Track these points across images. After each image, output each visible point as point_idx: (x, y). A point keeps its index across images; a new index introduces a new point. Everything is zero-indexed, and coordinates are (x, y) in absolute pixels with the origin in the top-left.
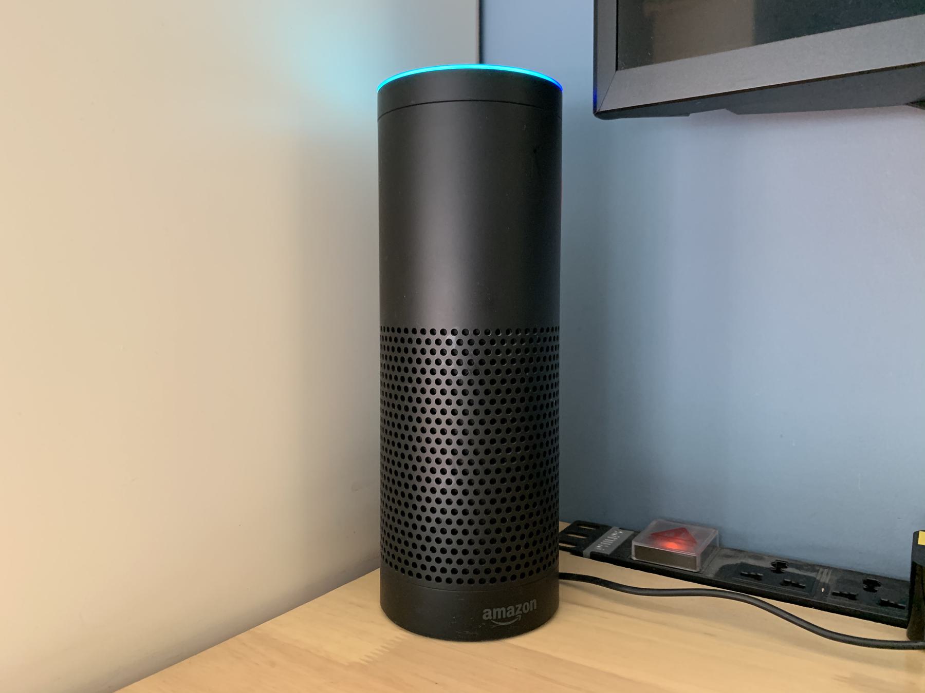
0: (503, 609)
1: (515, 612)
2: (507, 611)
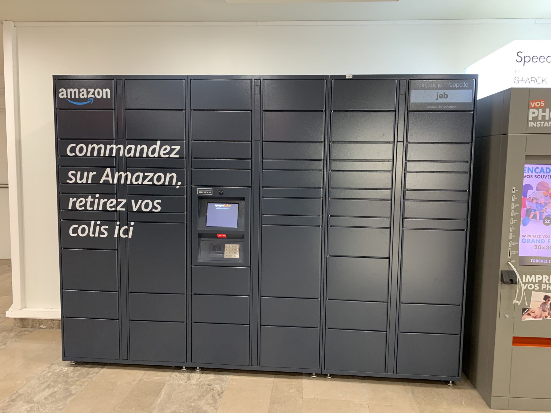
0: (76, 90)
1: (88, 94)
2: (79, 93)
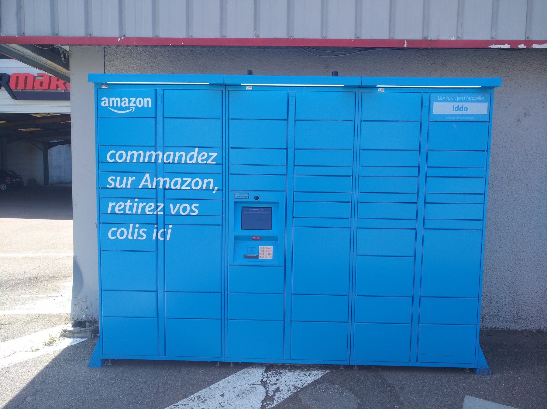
0: (118, 99)
1: (129, 103)
2: (121, 102)
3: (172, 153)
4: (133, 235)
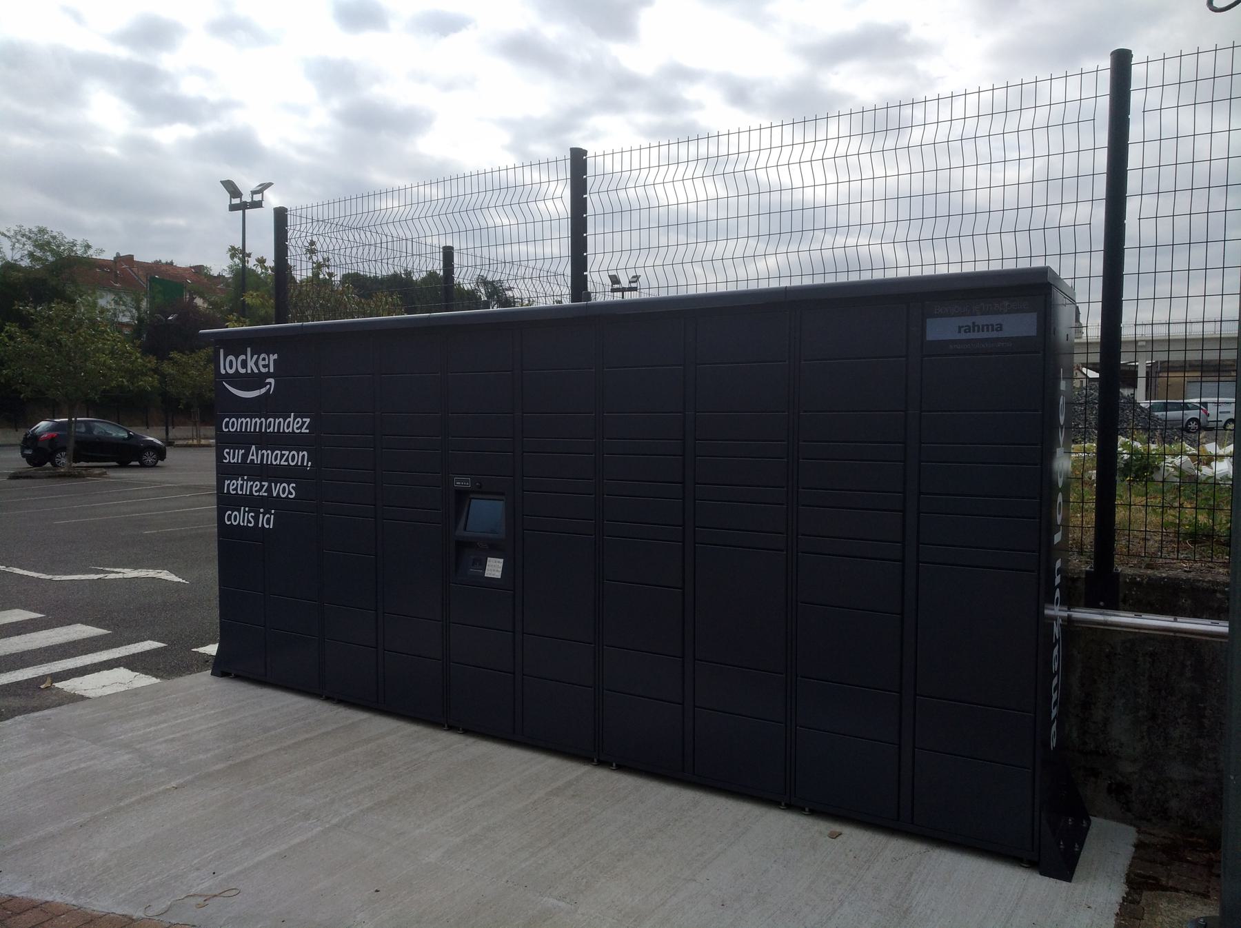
3: (272, 420)
4: (243, 522)
